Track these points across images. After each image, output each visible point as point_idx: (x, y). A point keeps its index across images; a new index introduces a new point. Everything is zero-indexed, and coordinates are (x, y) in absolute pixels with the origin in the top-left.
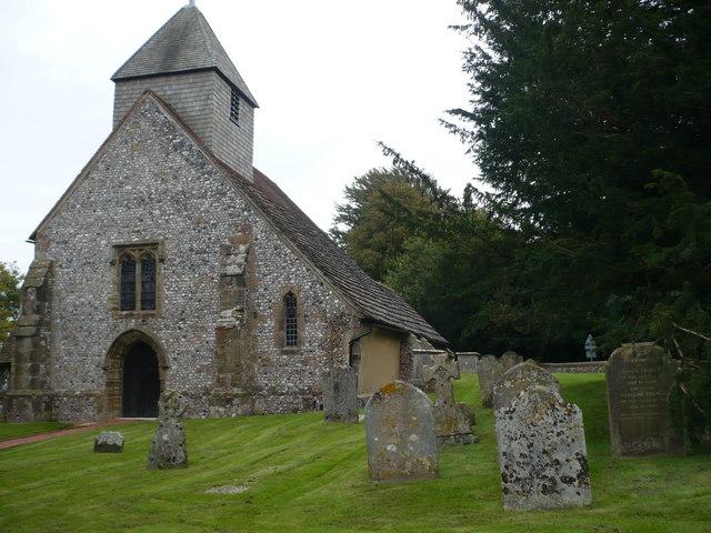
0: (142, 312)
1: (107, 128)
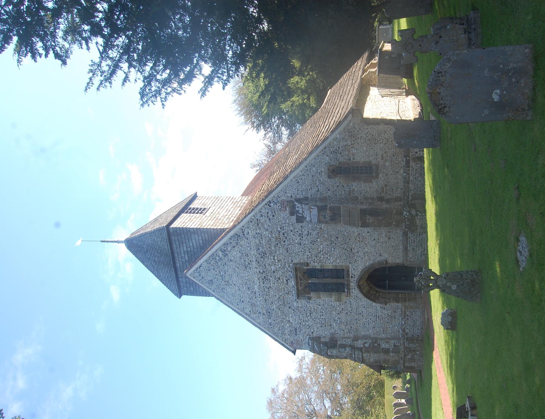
0: (346, 278)
1: (212, 301)
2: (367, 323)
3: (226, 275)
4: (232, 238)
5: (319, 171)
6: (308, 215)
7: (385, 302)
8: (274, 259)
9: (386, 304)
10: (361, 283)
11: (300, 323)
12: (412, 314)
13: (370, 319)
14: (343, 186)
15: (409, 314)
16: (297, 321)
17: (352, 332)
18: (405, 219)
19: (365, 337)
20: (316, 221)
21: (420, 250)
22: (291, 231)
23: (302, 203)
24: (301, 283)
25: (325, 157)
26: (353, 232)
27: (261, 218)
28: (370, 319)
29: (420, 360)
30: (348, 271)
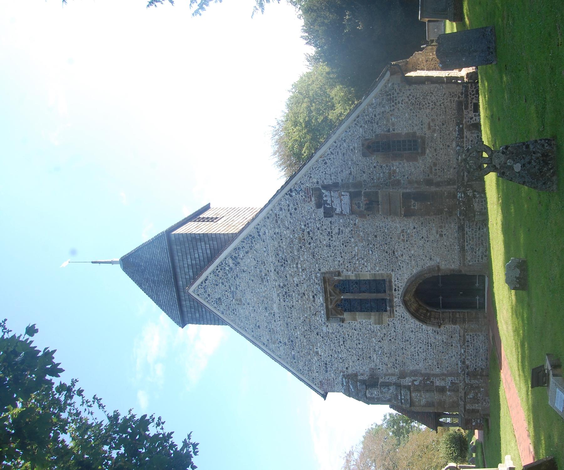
0: (388, 292)
2: (417, 354)
3: (237, 291)
4: (245, 241)
5: (351, 147)
6: (338, 205)
7: (438, 323)
8: (297, 267)
9: (440, 327)
10: (407, 298)
11: (332, 356)
12: (474, 340)
13: (420, 348)
14: (381, 167)
15: (469, 340)
16: (327, 353)
17: (398, 366)
18: (459, 203)
19: (415, 373)
20: (348, 211)
21: (481, 250)
22: (318, 229)
23: (330, 191)
24: (331, 299)
25: (358, 128)
26: (396, 227)
27: (281, 212)
28: (420, 348)
29: (485, 400)
30: (390, 282)
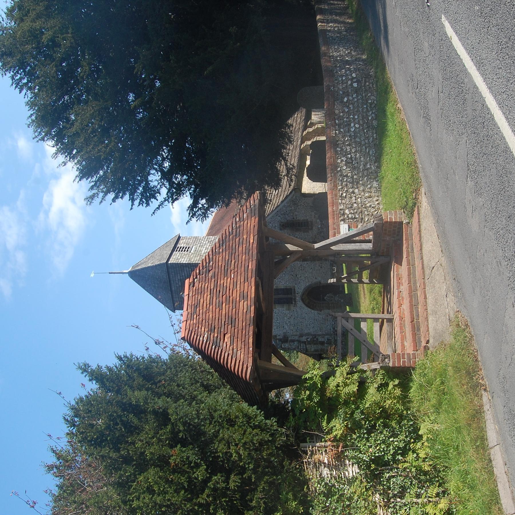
9: (321, 311)
19: (308, 334)
30: (295, 290)
